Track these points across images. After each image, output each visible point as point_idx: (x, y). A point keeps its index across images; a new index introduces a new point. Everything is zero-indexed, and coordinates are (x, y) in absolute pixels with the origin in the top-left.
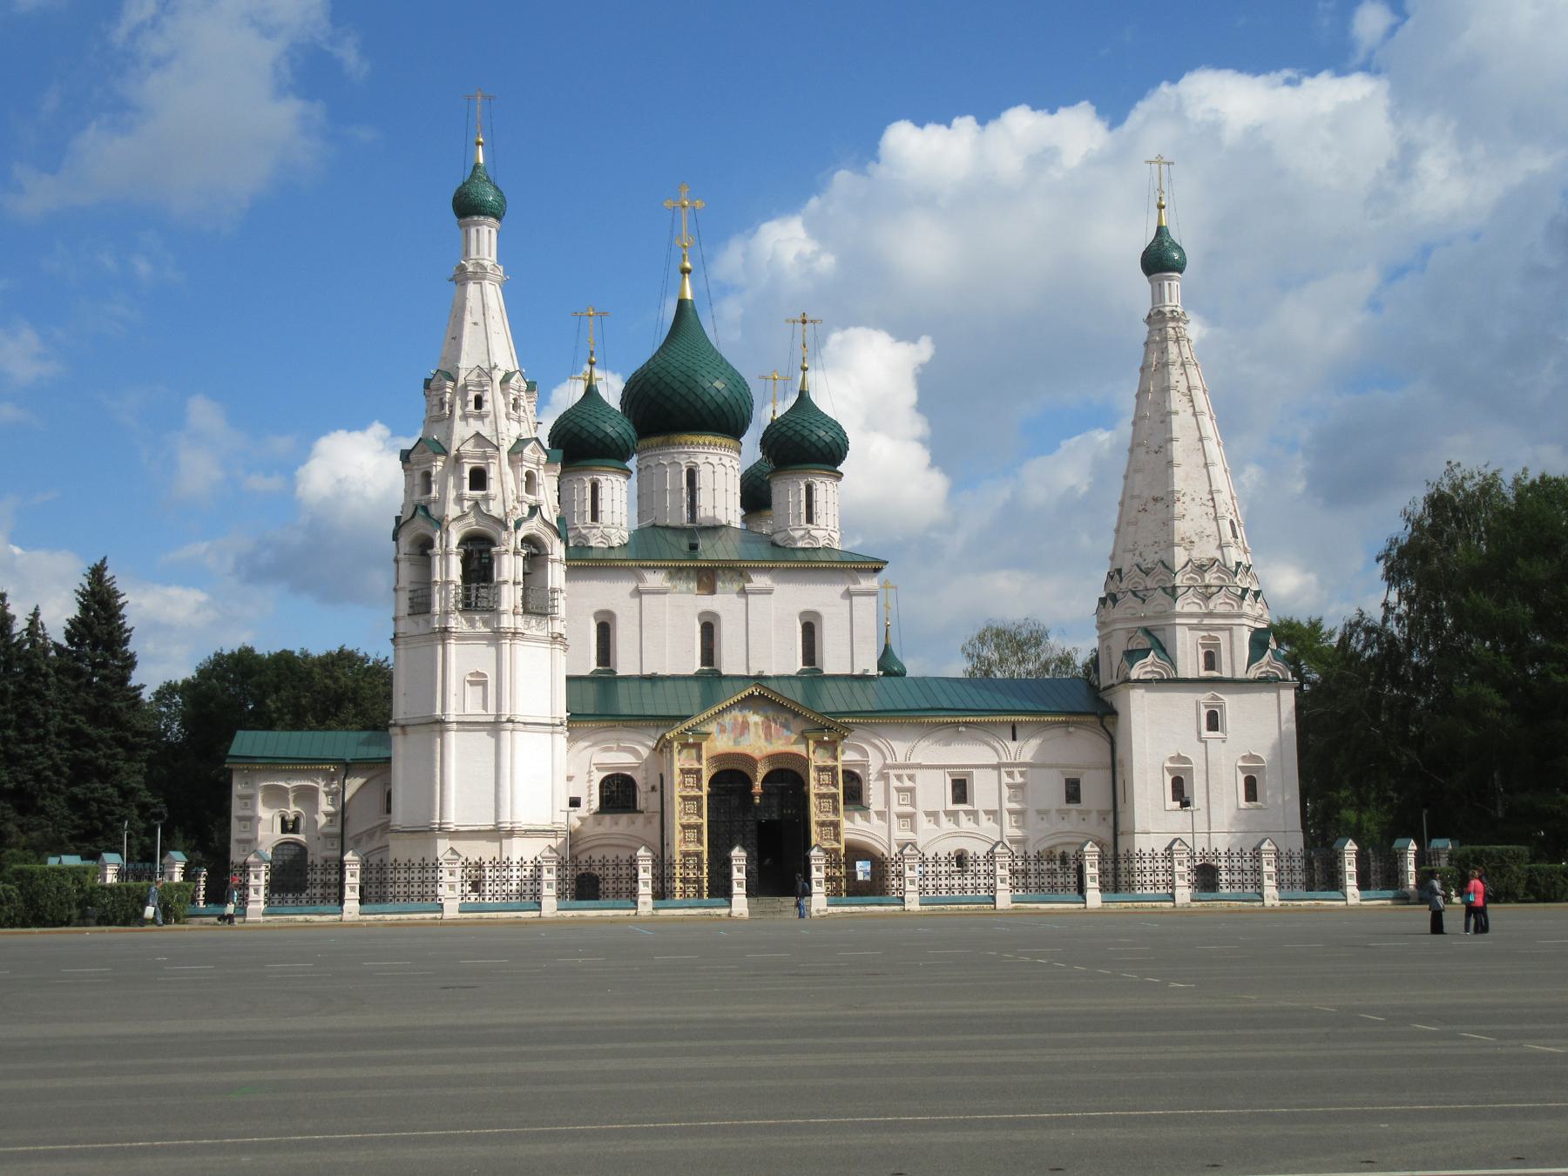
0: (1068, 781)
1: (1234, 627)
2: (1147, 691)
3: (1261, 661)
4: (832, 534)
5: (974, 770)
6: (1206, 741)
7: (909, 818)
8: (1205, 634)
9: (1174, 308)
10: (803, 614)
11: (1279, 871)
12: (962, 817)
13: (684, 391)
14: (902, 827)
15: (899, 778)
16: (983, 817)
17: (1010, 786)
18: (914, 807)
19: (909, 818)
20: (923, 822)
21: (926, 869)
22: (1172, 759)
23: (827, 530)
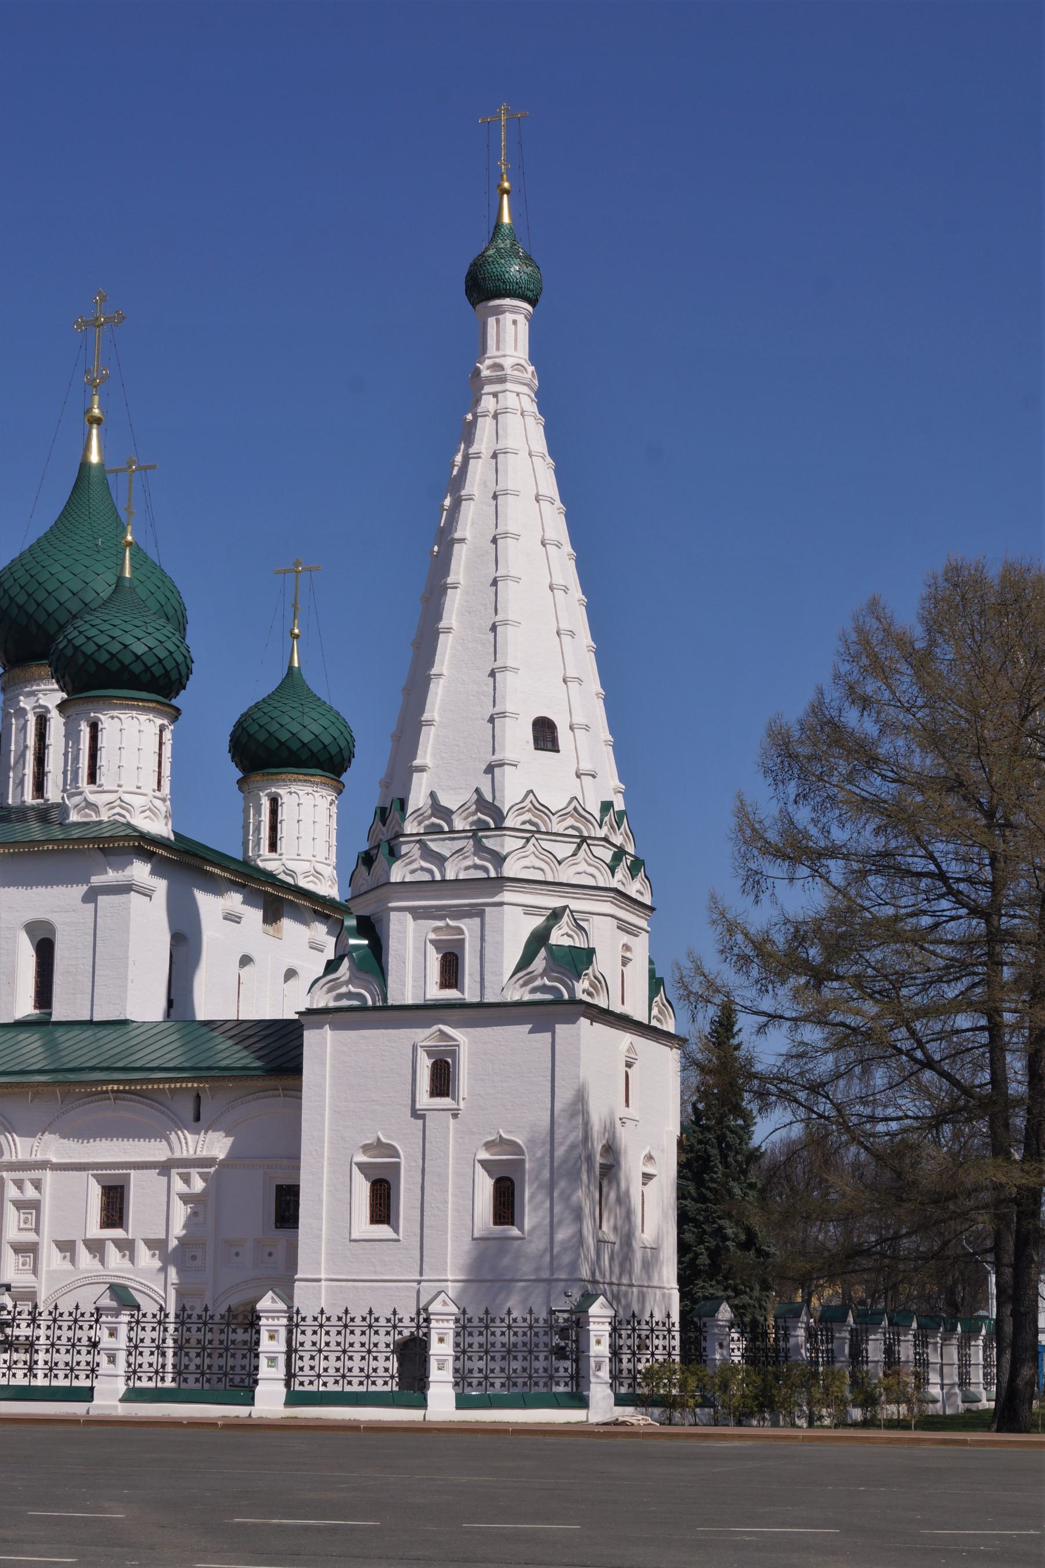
0: (279, 1188)
1: (487, 909)
2: (335, 1027)
3: (530, 969)
4: (127, 798)
5: (132, 1172)
6: (423, 1117)
7: (28, 1250)
8: (440, 924)
9: (497, 360)
10: (31, 928)
11: (134, 1348)
12: (112, 1251)
13: (21, 599)
14: (21, 1267)
15: (19, 1184)
16: (142, 1250)
17: (185, 1198)
18: (37, 1230)
19: (28, 1250)
20: (52, 1259)
21: (70, 1334)
22: (366, 1149)
23: (117, 792)
